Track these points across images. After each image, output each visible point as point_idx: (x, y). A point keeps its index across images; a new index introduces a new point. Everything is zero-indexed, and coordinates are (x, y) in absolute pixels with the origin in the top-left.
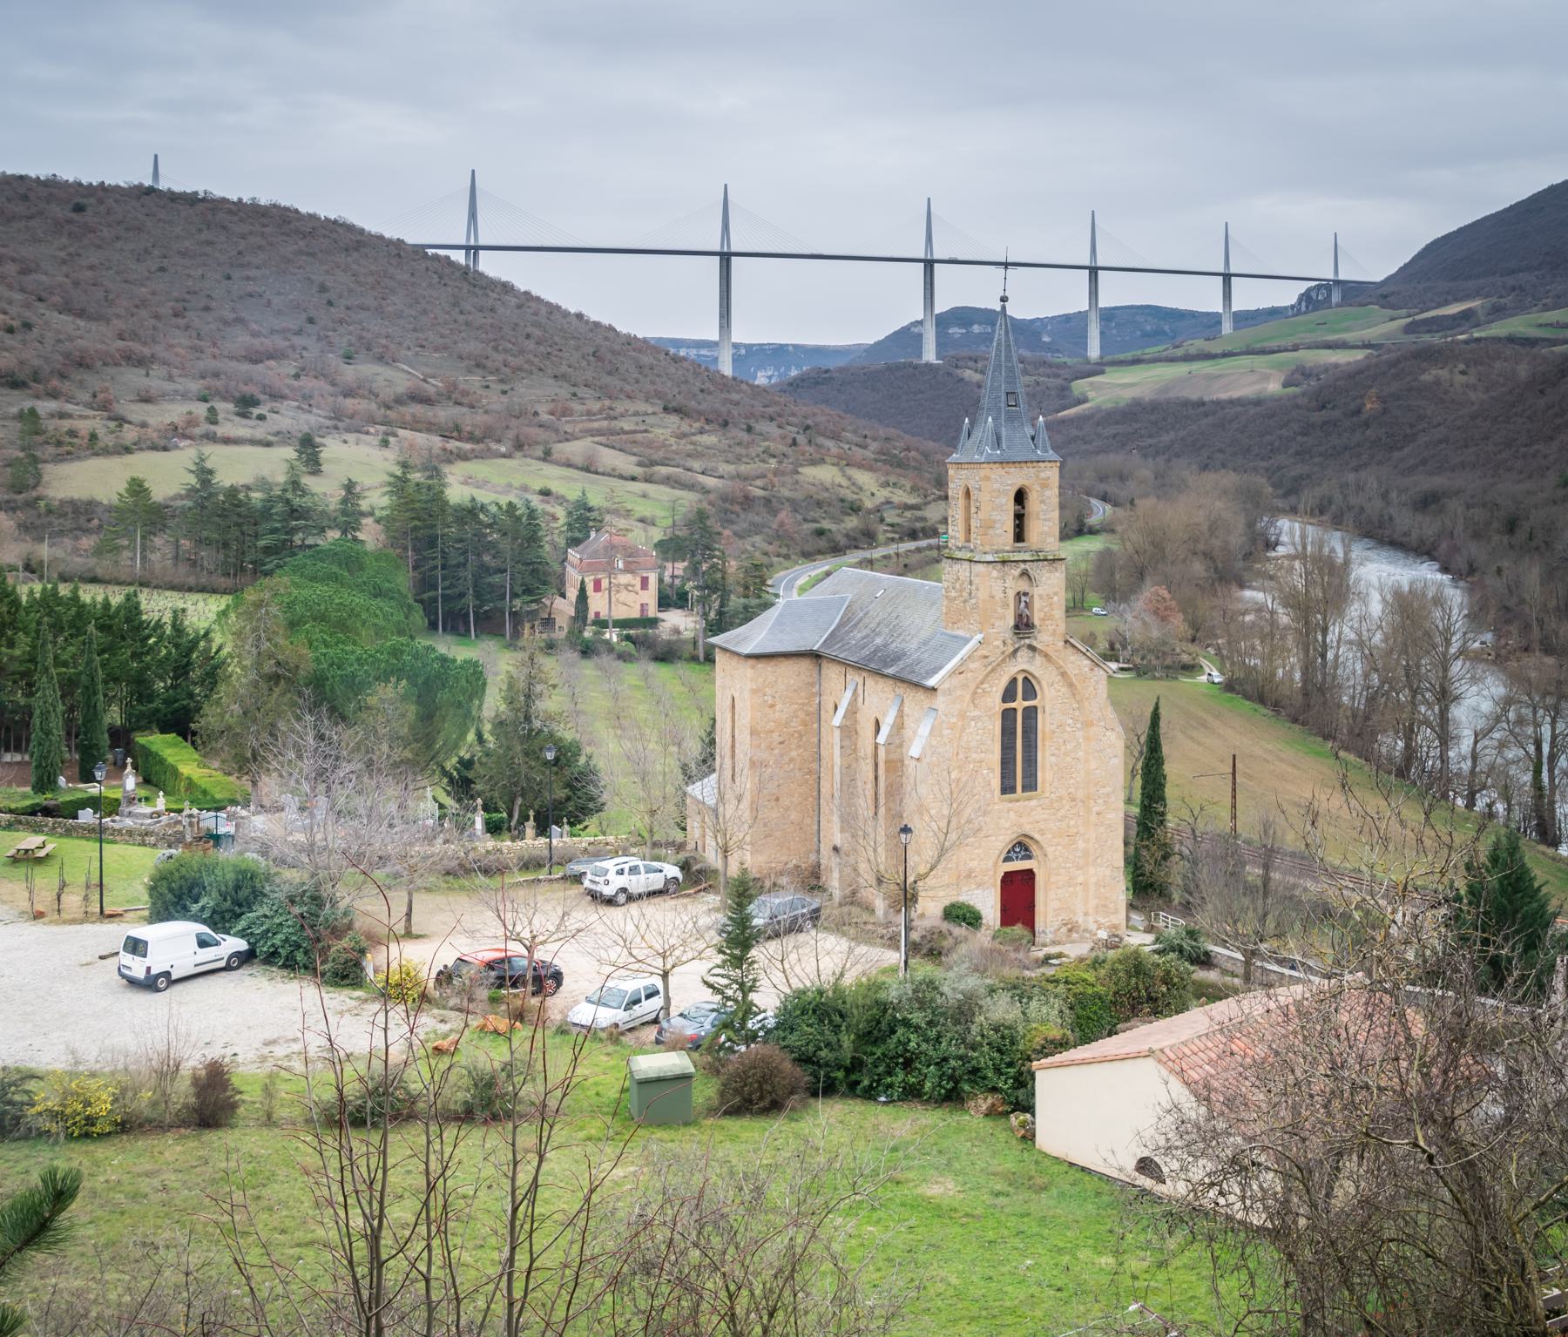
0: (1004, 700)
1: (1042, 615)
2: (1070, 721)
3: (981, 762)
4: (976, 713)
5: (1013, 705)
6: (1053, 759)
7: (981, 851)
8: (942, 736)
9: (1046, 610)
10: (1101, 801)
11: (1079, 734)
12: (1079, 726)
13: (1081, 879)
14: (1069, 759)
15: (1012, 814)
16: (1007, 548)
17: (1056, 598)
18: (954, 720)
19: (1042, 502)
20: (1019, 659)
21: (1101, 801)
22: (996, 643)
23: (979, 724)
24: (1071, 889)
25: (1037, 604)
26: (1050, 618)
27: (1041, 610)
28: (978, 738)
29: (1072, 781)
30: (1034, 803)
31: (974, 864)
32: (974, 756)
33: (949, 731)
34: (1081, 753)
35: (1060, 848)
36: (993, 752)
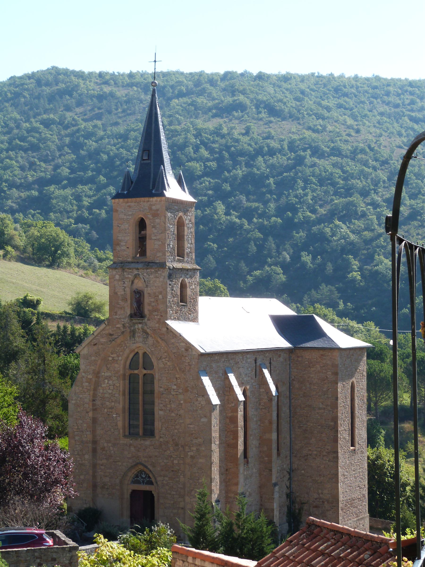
0: (131, 368)
1: (151, 308)
2: (175, 387)
3: (112, 408)
4: (108, 374)
5: (136, 372)
6: (161, 413)
7: (111, 471)
8: (83, 387)
9: (153, 304)
10: (194, 449)
11: (181, 397)
12: (180, 391)
13: (182, 505)
14: (173, 414)
15: (132, 449)
16: (130, 260)
17: (160, 297)
18: (90, 377)
19: (154, 227)
20: (137, 339)
21: (194, 449)
22: (118, 326)
23: (110, 382)
24: (175, 511)
25: (147, 300)
26: (157, 310)
27: (149, 304)
28: (110, 391)
29: (176, 431)
30: (148, 442)
31: (107, 480)
32: (108, 403)
33: (87, 384)
34: (182, 412)
35: (167, 479)
36: (119, 403)
